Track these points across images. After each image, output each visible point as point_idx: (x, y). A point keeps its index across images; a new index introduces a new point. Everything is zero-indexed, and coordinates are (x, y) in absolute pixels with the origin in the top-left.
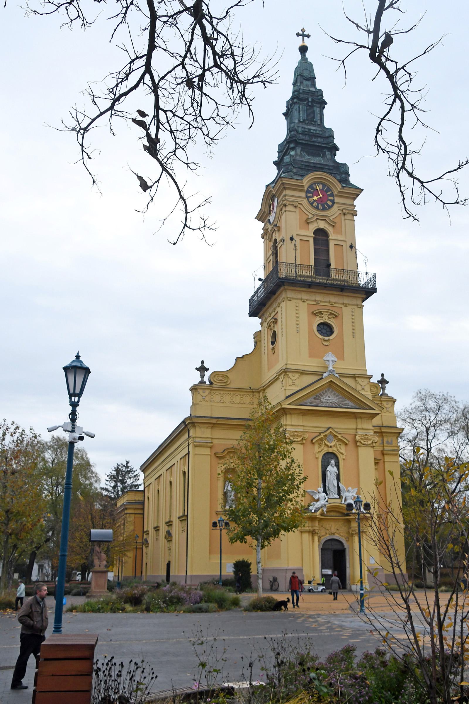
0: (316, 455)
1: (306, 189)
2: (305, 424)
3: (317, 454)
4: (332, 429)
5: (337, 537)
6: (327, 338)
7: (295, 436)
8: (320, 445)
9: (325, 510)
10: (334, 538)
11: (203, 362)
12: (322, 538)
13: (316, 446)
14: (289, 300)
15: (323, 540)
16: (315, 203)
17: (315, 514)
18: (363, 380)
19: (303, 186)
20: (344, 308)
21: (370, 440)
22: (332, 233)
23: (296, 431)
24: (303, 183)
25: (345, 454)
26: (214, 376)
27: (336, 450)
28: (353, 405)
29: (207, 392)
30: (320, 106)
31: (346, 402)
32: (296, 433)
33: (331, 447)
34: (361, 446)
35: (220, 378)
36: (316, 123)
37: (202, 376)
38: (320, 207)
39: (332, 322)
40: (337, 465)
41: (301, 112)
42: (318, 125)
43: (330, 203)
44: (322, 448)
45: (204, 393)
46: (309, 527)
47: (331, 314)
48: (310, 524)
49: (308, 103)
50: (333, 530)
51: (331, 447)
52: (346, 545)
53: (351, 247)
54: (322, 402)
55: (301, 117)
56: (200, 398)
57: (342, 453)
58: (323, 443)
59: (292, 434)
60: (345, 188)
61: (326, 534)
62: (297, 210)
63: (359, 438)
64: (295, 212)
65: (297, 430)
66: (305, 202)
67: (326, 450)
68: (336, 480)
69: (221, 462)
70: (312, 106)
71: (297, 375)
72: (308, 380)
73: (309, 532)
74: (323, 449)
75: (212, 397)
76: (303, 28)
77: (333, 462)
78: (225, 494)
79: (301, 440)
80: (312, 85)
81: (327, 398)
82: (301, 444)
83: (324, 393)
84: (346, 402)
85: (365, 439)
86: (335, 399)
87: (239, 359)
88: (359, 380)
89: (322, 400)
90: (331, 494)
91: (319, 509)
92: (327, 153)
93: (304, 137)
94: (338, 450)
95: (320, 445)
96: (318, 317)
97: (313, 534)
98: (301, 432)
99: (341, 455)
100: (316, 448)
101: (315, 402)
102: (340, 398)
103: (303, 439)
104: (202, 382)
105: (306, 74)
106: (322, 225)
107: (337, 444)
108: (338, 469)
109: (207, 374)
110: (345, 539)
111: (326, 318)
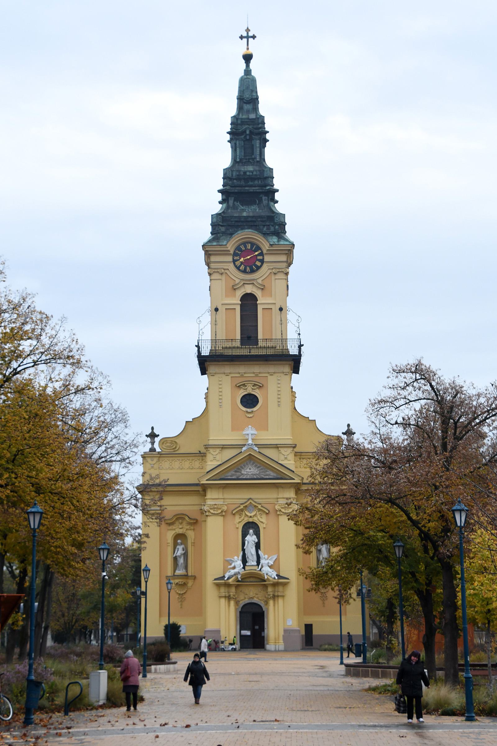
1: (232, 252)
3: (237, 525)
5: (255, 600)
6: (249, 410)
8: (240, 515)
9: (239, 576)
10: (253, 601)
11: (153, 428)
12: (241, 602)
13: (237, 517)
14: (212, 375)
15: (242, 603)
16: (243, 265)
18: (285, 449)
19: (229, 251)
20: (270, 378)
22: (261, 297)
23: (215, 505)
24: (227, 248)
26: (163, 443)
28: (275, 475)
29: (155, 460)
30: (260, 138)
31: (267, 473)
32: (215, 506)
35: (168, 444)
36: (255, 160)
37: (153, 443)
38: (248, 269)
39: (257, 393)
40: (257, 534)
41: (238, 150)
42: (258, 162)
43: (258, 263)
44: (242, 518)
45: (152, 461)
47: (255, 385)
49: (245, 137)
50: (252, 594)
51: (251, 517)
53: (281, 309)
54: (242, 474)
55: (238, 156)
56: (148, 466)
57: (262, 522)
58: (244, 514)
60: (273, 246)
61: (245, 598)
62: (224, 277)
63: (279, 508)
64: (221, 279)
66: (231, 266)
67: (246, 520)
68: (254, 548)
69: (170, 528)
70: (251, 140)
71: (218, 450)
72: (229, 454)
73: (225, 597)
74: (243, 519)
75: (161, 464)
76: (248, 28)
77: (251, 531)
78: (175, 559)
79: (221, 513)
80: (253, 108)
81: (248, 470)
83: (245, 466)
84: (267, 473)
86: (256, 470)
87: (188, 423)
88: (282, 450)
89: (243, 472)
91: (232, 576)
92: (264, 198)
93: (239, 183)
94: (258, 519)
95: (240, 515)
96: (242, 389)
98: (221, 505)
100: (237, 519)
101: (236, 475)
102: (262, 469)
103: (222, 511)
104: (152, 450)
105: (247, 96)
106: (249, 289)
107: (258, 513)
108: (258, 537)
109: (157, 440)
110: (263, 603)
111: (250, 390)
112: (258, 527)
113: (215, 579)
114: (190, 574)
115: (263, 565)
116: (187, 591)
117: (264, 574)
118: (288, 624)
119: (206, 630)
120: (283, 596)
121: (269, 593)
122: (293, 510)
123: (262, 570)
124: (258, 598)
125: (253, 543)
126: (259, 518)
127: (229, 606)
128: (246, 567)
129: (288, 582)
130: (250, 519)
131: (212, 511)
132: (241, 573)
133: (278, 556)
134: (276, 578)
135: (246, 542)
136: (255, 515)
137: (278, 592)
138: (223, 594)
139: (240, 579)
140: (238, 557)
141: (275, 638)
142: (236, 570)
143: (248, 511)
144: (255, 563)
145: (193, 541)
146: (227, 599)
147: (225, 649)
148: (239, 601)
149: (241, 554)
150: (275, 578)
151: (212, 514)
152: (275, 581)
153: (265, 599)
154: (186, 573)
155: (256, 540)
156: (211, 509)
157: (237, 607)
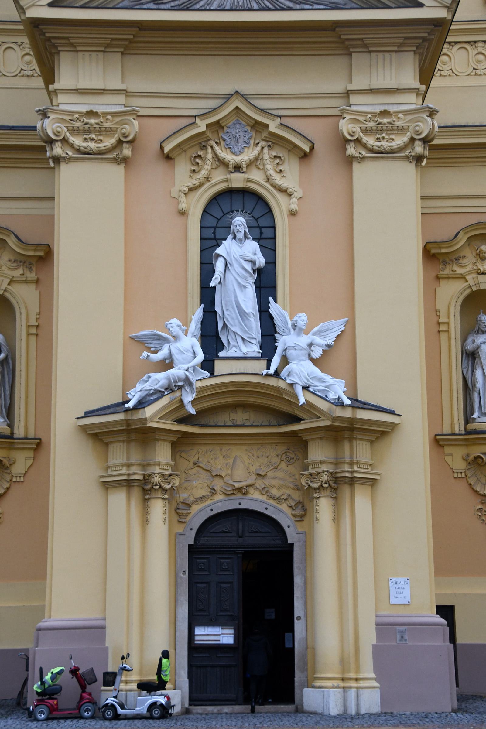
0: (179, 202)
2: (134, 86)
3: (183, 199)
4: (245, 98)
7: (89, 131)
9: (188, 397)
10: (245, 505)
12: (195, 508)
17: (139, 415)
21: (401, 130)
23: (90, 114)
25: (298, 193)
27: (263, 182)
32: (93, 121)
33: (238, 168)
34: (364, 158)
46: (129, 466)
48: (136, 456)
51: (238, 168)
52: (292, 536)
57: (284, 191)
58: (210, 156)
59: (78, 124)
61: (213, 491)
65: (99, 109)
68: (251, 291)
73: (129, 484)
74: (207, 179)
79: (113, 148)
82: (116, 160)
85: (382, 131)
90: (232, 343)
91: (159, 394)
95: (196, 160)
97: (145, 492)
98: (115, 114)
99: (280, 197)
103: (120, 142)
107: (266, 156)
110: (289, 511)
112: (270, 211)
113: (88, 414)
114: (19, 432)
115: (291, 353)
116: (8, 489)
117: (291, 385)
118: (393, 601)
119: (42, 624)
120: (372, 483)
121: (311, 471)
122: (412, 140)
123: (283, 374)
124: (264, 491)
125: (248, 267)
126: (272, 172)
127: (145, 521)
128: (217, 363)
129: (394, 426)
131: (77, 141)
132: (199, 384)
133: (351, 324)
134: (347, 402)
135: (219, 266)
136: (256, 159)
137: (351, 464)
138: (122, 473)
139: (193, 411)
140: (186, 323)
141: (343, 661)
142: (177, 372)
143: (228, 147)
144: (254, 349)
145: (33, 322)
146: (136, 492)
147: (120, 711)
148: (189, 506)
149: (198, 313)
150: (341, 404)
151: (79, 151)
152: (339, 413)
153: (296, 496)
154: (7, 430)
155: (261, 261)
156: (74, 131)
157: (180, 529)
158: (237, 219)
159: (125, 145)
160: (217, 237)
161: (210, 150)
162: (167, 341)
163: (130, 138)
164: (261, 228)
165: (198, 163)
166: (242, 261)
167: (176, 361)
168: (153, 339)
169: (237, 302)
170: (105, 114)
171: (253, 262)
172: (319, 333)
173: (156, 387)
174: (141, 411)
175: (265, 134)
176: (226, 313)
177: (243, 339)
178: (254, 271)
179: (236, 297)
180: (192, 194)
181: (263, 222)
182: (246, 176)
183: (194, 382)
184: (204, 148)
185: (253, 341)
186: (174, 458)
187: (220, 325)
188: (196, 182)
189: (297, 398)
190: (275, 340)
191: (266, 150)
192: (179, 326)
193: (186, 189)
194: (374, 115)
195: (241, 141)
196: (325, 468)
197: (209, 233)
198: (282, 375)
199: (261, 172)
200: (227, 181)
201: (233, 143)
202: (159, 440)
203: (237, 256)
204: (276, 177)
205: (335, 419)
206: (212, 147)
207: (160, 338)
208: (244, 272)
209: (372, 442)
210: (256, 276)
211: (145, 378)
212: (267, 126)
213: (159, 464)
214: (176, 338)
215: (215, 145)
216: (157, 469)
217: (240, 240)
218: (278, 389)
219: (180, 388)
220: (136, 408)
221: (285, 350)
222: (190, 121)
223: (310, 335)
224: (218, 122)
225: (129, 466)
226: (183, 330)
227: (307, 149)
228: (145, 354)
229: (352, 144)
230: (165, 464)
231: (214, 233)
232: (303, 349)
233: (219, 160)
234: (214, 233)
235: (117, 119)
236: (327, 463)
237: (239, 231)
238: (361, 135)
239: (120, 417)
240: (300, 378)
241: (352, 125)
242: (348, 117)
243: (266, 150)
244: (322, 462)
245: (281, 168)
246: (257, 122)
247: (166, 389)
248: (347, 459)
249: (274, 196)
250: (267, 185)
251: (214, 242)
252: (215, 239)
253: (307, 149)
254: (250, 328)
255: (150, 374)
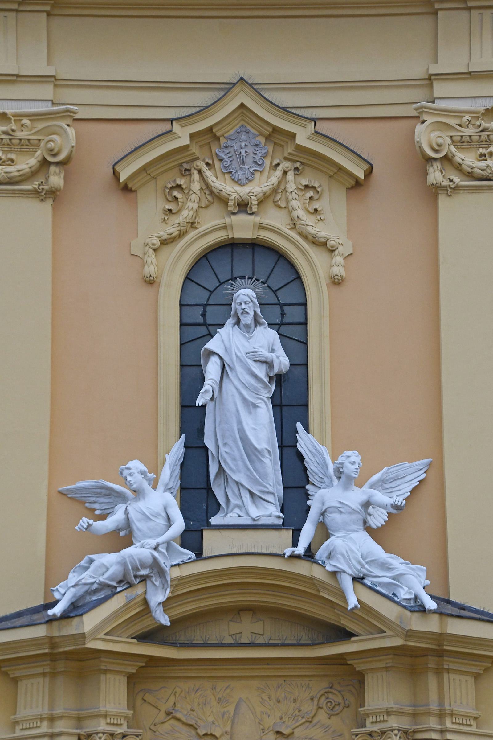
0: (144, 264)
3: (151, 257)
34: (457, 189)
44: (186, 214)
46: (52, 719)
58: (196, 186)
74: (192, 225)
79: (33, 174)
90: (234, 501)
98: (35, 117)
103: (45, 163)
107: (291, 187)
115: (333, 518)
117: (334, 574)
121: (370, 727)
123: (321, 554)
125: (261, 372)
126: (300, 213)
128: (207, 535)
130: (242, 218)
132: (176, 573)
134: (431, 605)
136: (275, 191)
137: (441, 716)
139: (165, 620)
150: (422, 609)
158: (242, 291)
159: (53, 169)
160: (209, 321)
161: (196, 176)
162: (121, 498)
163: (61, 157)
164: (282, 305)
165: (176, 198)
166: (250, 362)
167: (137, 533)
168: (99, 495)
169: (242, 431)
170: (19, 116)
171: (269, 364)
172: (381, 485)
173: (102, 579)
174: (76, 620)
175: (289, 149)
176: (223, 449)
177: (251, 493)
178: (271, 379)
179: (240, 422)
180: (166, 250)
181: (285, 296)
182: (257, 219)
183: (167, 569)
184: (187, 172)
185: (270, 498)
186: (131, 705)
187: (213, 470)
188: (175, 231)
189: (344, 598)
190: (307, 496)
191: (290, 176)
192: (142, 473)
193: (157, 242)
194: (475, 115)
195: (249, 160)
196: (393, 722)
197: (195, 315)
198: (317, 556)
199: (284, 212)
200: (225, 227)
201: (235, 165)
202: (106, 671)
203: (242, 354)
204: (308, 220)
205: (409, 634)
206: (200, 171)
207: (110, 493)
208: (252, 381)
209: (477, 677)
210: (273, 387)
211: (83, 563)
212: (293, 136)
213: (105, 716)
214: (138, 493)
215: (204, 168)
216: (102, 725)
217: (247, 327)
218: (311, 581)
219: (144, 579)
220: (65, 616)
221: (323, 514)
222: (164, 127)
223: (365, 488)
224: (210, 130)
225: (52, 719)
226: (149, 480)
227: (361, 175)
228: (84, 521)
229: (437, 165)
230: (117, 716)
231: (204, 315)
232: (354, 511)
233: (212, 193)
234: (204, 315)
235: (40, 125)
236: (399, 713)
237: (244, 312)
238: (453, 149)
239: (40, 631)
240: (348, 562)
241: (437, 133)
242: (430, 120)
243: (290, 176)
244: (389, 713)
245: (316, 205)
246: (275, 130)
247: (120, 582)
248: (434, 707)
249: (304, 253)
250: (293, 234)
251: (203, 331)
252: (205, 324)
253: (361, 175)
254: (264, 476)
255: (92, 556)
